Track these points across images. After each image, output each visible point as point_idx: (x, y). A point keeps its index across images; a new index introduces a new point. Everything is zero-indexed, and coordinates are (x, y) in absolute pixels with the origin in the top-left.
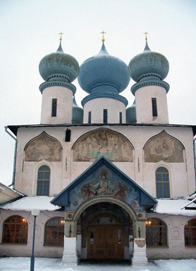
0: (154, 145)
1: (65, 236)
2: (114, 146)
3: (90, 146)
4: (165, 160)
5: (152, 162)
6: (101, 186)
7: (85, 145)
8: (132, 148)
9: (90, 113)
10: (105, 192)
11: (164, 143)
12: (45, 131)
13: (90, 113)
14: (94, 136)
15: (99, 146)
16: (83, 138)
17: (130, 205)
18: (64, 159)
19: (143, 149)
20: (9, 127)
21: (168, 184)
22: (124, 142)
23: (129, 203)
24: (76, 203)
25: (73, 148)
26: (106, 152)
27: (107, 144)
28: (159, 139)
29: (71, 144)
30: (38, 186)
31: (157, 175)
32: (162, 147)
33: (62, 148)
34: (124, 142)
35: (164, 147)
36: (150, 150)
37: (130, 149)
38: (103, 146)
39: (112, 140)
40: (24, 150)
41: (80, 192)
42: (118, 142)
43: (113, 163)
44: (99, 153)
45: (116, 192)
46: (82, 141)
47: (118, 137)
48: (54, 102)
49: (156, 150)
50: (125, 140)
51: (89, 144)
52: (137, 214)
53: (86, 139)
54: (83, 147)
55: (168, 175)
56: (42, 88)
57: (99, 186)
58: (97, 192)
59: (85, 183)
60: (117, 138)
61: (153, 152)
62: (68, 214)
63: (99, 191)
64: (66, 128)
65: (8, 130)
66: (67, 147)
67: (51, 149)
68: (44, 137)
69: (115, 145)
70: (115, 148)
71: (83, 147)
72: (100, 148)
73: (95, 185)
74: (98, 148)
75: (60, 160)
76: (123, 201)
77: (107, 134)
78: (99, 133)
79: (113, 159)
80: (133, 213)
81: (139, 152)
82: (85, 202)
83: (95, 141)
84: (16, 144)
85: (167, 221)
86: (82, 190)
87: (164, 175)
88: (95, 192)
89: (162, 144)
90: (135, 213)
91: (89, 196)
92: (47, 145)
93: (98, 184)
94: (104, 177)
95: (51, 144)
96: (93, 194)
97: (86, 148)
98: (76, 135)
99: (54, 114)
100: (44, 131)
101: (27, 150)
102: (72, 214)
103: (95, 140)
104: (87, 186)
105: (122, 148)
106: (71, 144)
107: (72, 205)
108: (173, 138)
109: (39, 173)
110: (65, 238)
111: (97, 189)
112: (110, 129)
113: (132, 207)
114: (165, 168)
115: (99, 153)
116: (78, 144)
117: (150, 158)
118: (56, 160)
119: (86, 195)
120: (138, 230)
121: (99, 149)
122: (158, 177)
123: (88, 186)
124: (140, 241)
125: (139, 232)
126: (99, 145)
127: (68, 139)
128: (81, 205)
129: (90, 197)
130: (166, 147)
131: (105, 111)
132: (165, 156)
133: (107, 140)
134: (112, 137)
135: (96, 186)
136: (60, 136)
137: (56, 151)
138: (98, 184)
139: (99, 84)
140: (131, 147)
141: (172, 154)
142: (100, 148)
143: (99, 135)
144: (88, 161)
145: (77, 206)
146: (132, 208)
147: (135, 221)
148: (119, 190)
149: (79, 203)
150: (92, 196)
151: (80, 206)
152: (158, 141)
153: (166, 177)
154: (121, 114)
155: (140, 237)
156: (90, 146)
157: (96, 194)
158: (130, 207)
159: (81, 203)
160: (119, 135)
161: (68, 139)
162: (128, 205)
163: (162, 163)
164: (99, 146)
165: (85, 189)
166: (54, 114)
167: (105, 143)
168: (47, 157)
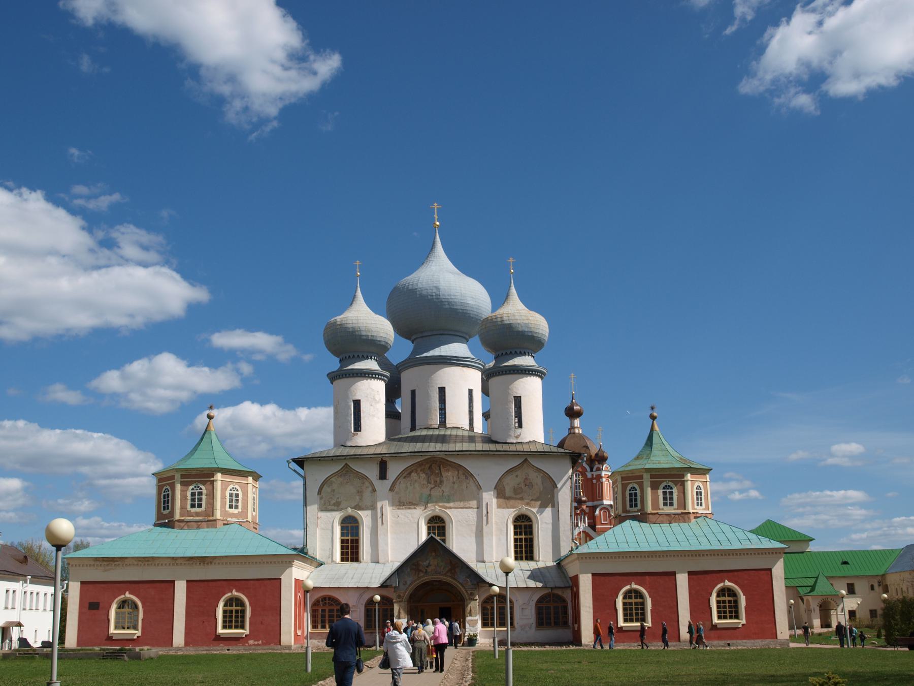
0: (510, 484)
1: (395, 618)
2: (452, 484)
3: (417, 485)
5: (508, 508)
6: (431, 563)
9: (413, 393)
10: (434, 570)
11: (526, 479)
12: (348, 463)
13: (413, 393)
14: (421, 471)
15: (431, 486)
16: (406, 474)
17: (460, 583)
19: (495, 489)
20: (295, 461)
21: (531, 540)
22: (467, 478)
23: (461, 582)
25: (391, 489)
26: (441, 494)
27: (441, 482)
28: (519, 473)
29: (388, 483)
32: (522, 486)
33: (374, 490)
34: (467, 478)
35: (526, 485)
36: (505, 490)
37: (474, 488)
38: (436, 486)
39: (449, 475)
40: (318, 494)
41: (409, 570)
42: (459, 478)
43: (448, 511)
44: (430, 495)
45: (447, 569)
46: (405, 477)
47: (458, 471)
49: (514, 489)
50: (468, 475)
51: (416, 481)
52: (469, 592)
53: (410, 474)
54: (407, 487)
55: (531, 527)
56: (334, 377)
57: (429, 563)
58: (426, 569)
60: (457, 472)
62: (397, 594)
63: (429, 570)
64: (380, 459)
65: (294, 466)
66: (383, 487)
67: (358, 492)
68: (346, 471)
69: (454, 483)
70: (453, 488)
71: (407, 487)
72: (432, 488)
73: (425, 563)
74: (429, 488)
76: (454, 579)
77: (441, 466)
78: (429, 465)
80: (465, 592)
82: (416, 581)
83: (424, 478)
84: (305, 485)
87: (526, 527)
88: (424, 571)
90: (467, 592)
91: (418, 574)
93: (428, 562)
94: (434, 554)
96: (423, 572)
98: (394, 470)
100: (346, 464)
101: (322, 494)
102: (402, 595)
103: (423, 475)
104: (416, 564)
106: (388, 483)
108: (539, 470)
111: (427, 567)
112: (446, 458)
113: (465, 585)
114: (526, 516)
115: (430, 495)
116: (398, 483)
119: (416, 573)
120: (469, 609)
121: (430, 490)
122: (517, 530)
124: (472, 620)
125: (471, 611)
126: (430, 483)
127: (383, 476)
128: (411, 584)
129: (420, 576)
133: (441, 474)
134: (448, 470)
135: (425, 564)
136: (372, 472)
137: (367, 493)
138: (428, 562)
140: (477, 486)
141: (538, 494)
142: (432, 488)
143: (430, 468)
145: (407, 586)
146: (463, 586)
147: (467, 600)
148: (450, 567)
149: (408, 583)
150: (422, 574)
151: (409, 586)
152: (517, 476)
154: (470, 391)
155: (471, 615)
156: (417, 485)
157: (426, 572)
158: (462, 585)
161: (383, 476)
162: (460, 583)
164: (429, 484)
165: (414, 567)
167: (438, 481)
168: (353, 505)
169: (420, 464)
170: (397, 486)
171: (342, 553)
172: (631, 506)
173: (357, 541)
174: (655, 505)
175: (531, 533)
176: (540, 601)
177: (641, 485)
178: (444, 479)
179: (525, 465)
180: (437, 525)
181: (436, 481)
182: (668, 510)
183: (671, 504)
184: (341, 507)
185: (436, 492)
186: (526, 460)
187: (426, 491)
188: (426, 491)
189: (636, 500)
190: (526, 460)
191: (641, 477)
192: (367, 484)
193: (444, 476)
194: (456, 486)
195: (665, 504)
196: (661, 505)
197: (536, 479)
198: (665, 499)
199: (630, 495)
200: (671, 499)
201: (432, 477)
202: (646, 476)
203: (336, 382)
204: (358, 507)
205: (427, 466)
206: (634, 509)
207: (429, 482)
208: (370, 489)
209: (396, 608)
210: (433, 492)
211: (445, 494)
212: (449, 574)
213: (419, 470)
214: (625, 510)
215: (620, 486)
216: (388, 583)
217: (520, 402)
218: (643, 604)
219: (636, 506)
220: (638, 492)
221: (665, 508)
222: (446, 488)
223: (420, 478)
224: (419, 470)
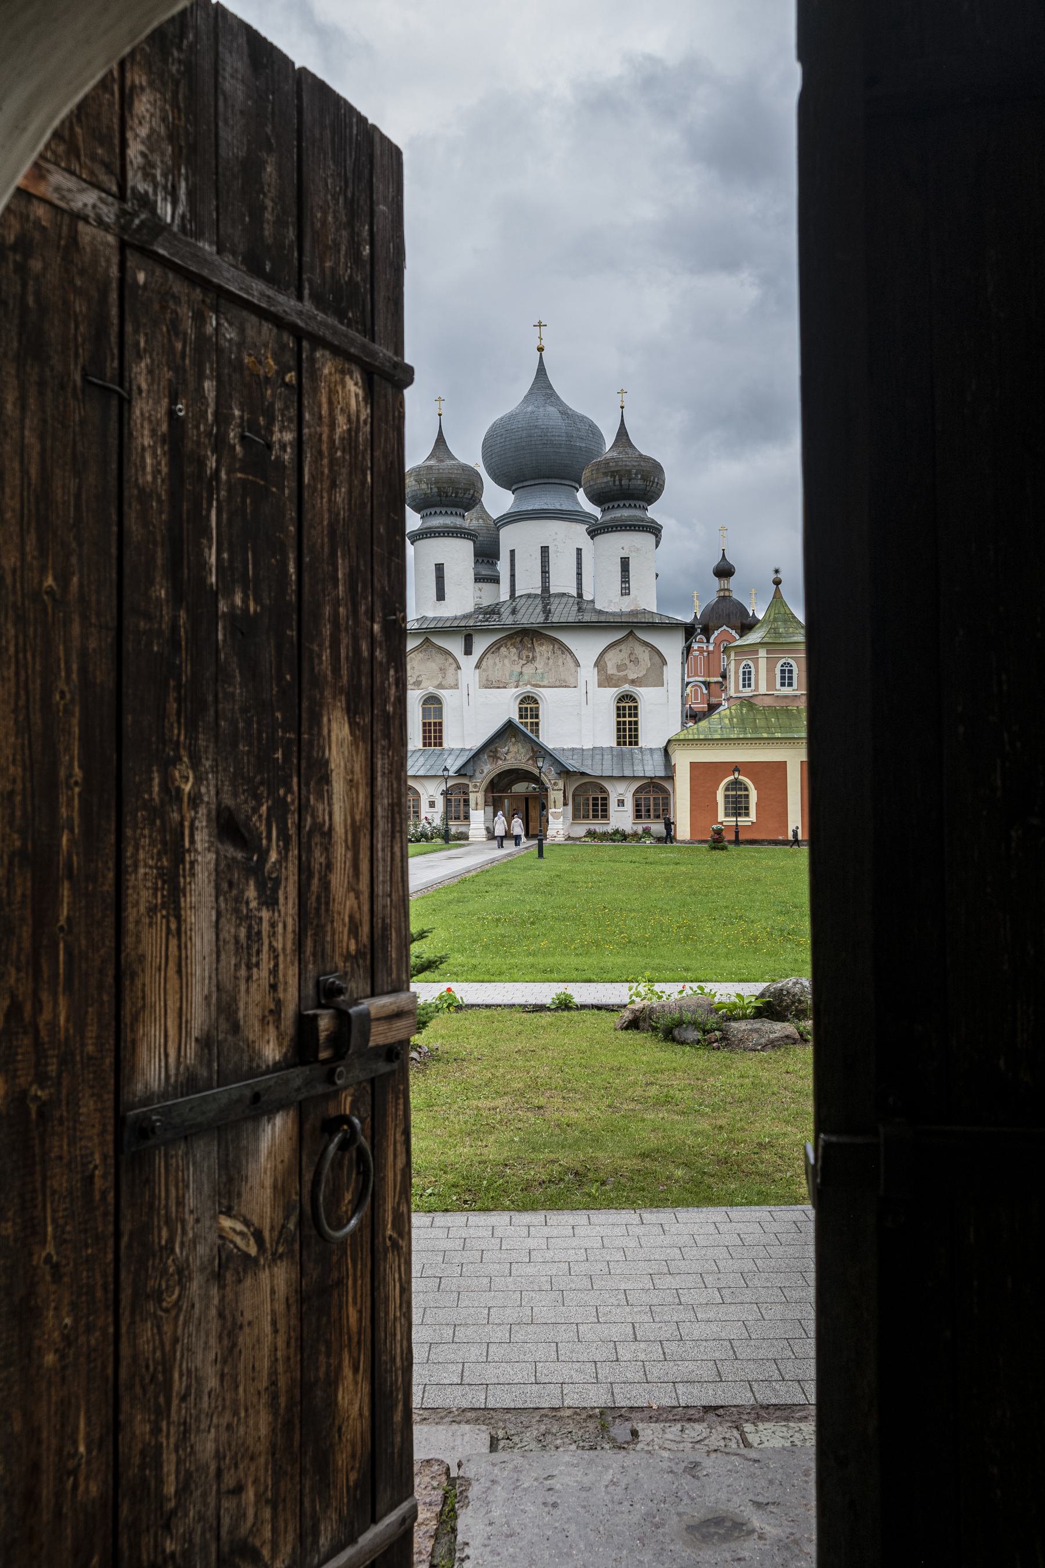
0: (612, 660)
4: (633, 682)
7: (497, 661)
8: (578, 664)
9: (512, 552)
10: (515, 756)
13: (512, 552)
16: (493, 648)
18: (463, 685)
19: (596, 664)
21: (636, 723)
22: (563, 653)
24: (482, 772)
25: (478, 667)
27: (533, 658)
28: (623, 647)
30: (424, 731)
31: (618, 708)
32: (627, 662)
33: (459, 668)
39: (543, 650)
44: (521, 673)
48: (440, 568)
51: (506, 657)
53: (499, 648)
55: (636, 708)
59: (492, 747)
61: (611, 670)
66: (468, 663)
75: (456, 686)
79: (545, 683)
81: (588, 673)
85: (607, 785)
86: (489, 756)
89: (627, 656)
92: (434, 661)
95: (439, 659)
97: (499, 665)
98: (480, 645)
99: (441, 596)
103: (514, 650)
105: (560, 663)
107: (477, 774)
108: (646, 644)
109: (424, 710)
110: (471, 812)
115: (521, 673)
117: (606, 681)
118: (452, 688)
122: (620, 712)
123: (496, 751)
127: (468, 651)
130: (635, 661)
131: (545, 550)
132: (632, 676)
134: (541, 645)
136: (455, 647)
137: (451, 670)
139: (532, 482)
144: (505, 687)
149: (485, 772)
150: (500, 762)
153: (634, 711)
156: (506, 661)
159: (488, 770)
160: (555, 640)
161: (468, 651)
163: (626, 687)
166: (441, 596)
168: (436, 683)
169: (509, 637)
170: (484, 663)
171: (424, 738)
172: (744, 686)
173: (440, 724)
174: (770, 684)
175: (636, 715)
176: (637, 792)
177: (756, 661)
178: (538, 655)
179: (630, 638)
180: (529, 706)
181: (528, 657)
182: (786, 691)
183: (790, 685)
184: (423, 685)
185: (528, 670)
186: (631, 633)
187: (517, 669)
188: (517, 669)
189: (749, 679)
190: (631, 633)
191: (756, 653)
192: (451, 660)
193: (537, 650)
194: (551, 661)
195: (783, 684)
196: (778, 686)
197: (644, 655)
198: (783, 678)
199: (744, 673)
200: (791, 678)
201: (525, 653)
202: (762, 653)
203: (417, 543)
204: (440, 686)
205: (518, 639)
206: (747, 689)
207: (519, 658)
208: (455, 666)
209: (472, 797)
210: (525, 670)
211: (539, 671)
212: (530, 762)
213: (509, 644)
214: (737, 691)
215: (733, 662)
216: (462, 772)
217: (628, 564)
218: (747, 796)
219: (750, 686)
220: (753, 670)
221: (783, 688)
222: (540, 664)
223: (510, 653)
224: (509, 644)
